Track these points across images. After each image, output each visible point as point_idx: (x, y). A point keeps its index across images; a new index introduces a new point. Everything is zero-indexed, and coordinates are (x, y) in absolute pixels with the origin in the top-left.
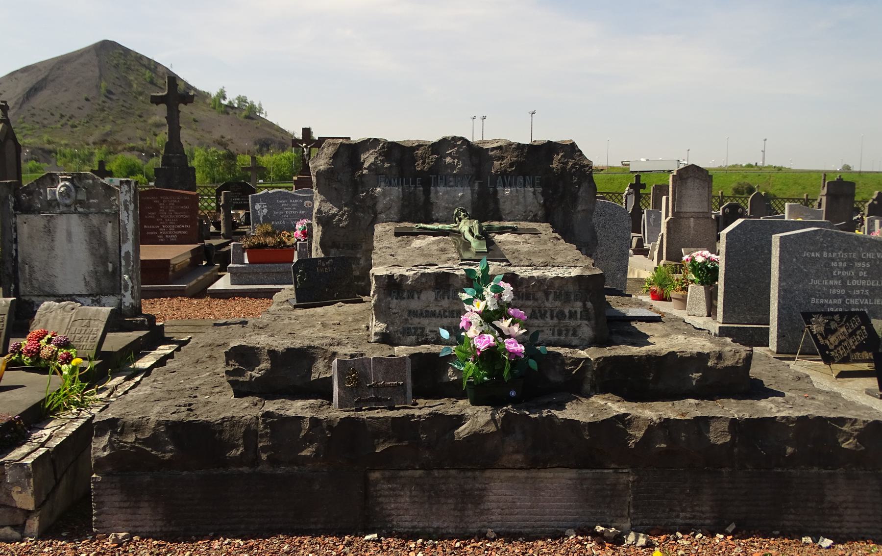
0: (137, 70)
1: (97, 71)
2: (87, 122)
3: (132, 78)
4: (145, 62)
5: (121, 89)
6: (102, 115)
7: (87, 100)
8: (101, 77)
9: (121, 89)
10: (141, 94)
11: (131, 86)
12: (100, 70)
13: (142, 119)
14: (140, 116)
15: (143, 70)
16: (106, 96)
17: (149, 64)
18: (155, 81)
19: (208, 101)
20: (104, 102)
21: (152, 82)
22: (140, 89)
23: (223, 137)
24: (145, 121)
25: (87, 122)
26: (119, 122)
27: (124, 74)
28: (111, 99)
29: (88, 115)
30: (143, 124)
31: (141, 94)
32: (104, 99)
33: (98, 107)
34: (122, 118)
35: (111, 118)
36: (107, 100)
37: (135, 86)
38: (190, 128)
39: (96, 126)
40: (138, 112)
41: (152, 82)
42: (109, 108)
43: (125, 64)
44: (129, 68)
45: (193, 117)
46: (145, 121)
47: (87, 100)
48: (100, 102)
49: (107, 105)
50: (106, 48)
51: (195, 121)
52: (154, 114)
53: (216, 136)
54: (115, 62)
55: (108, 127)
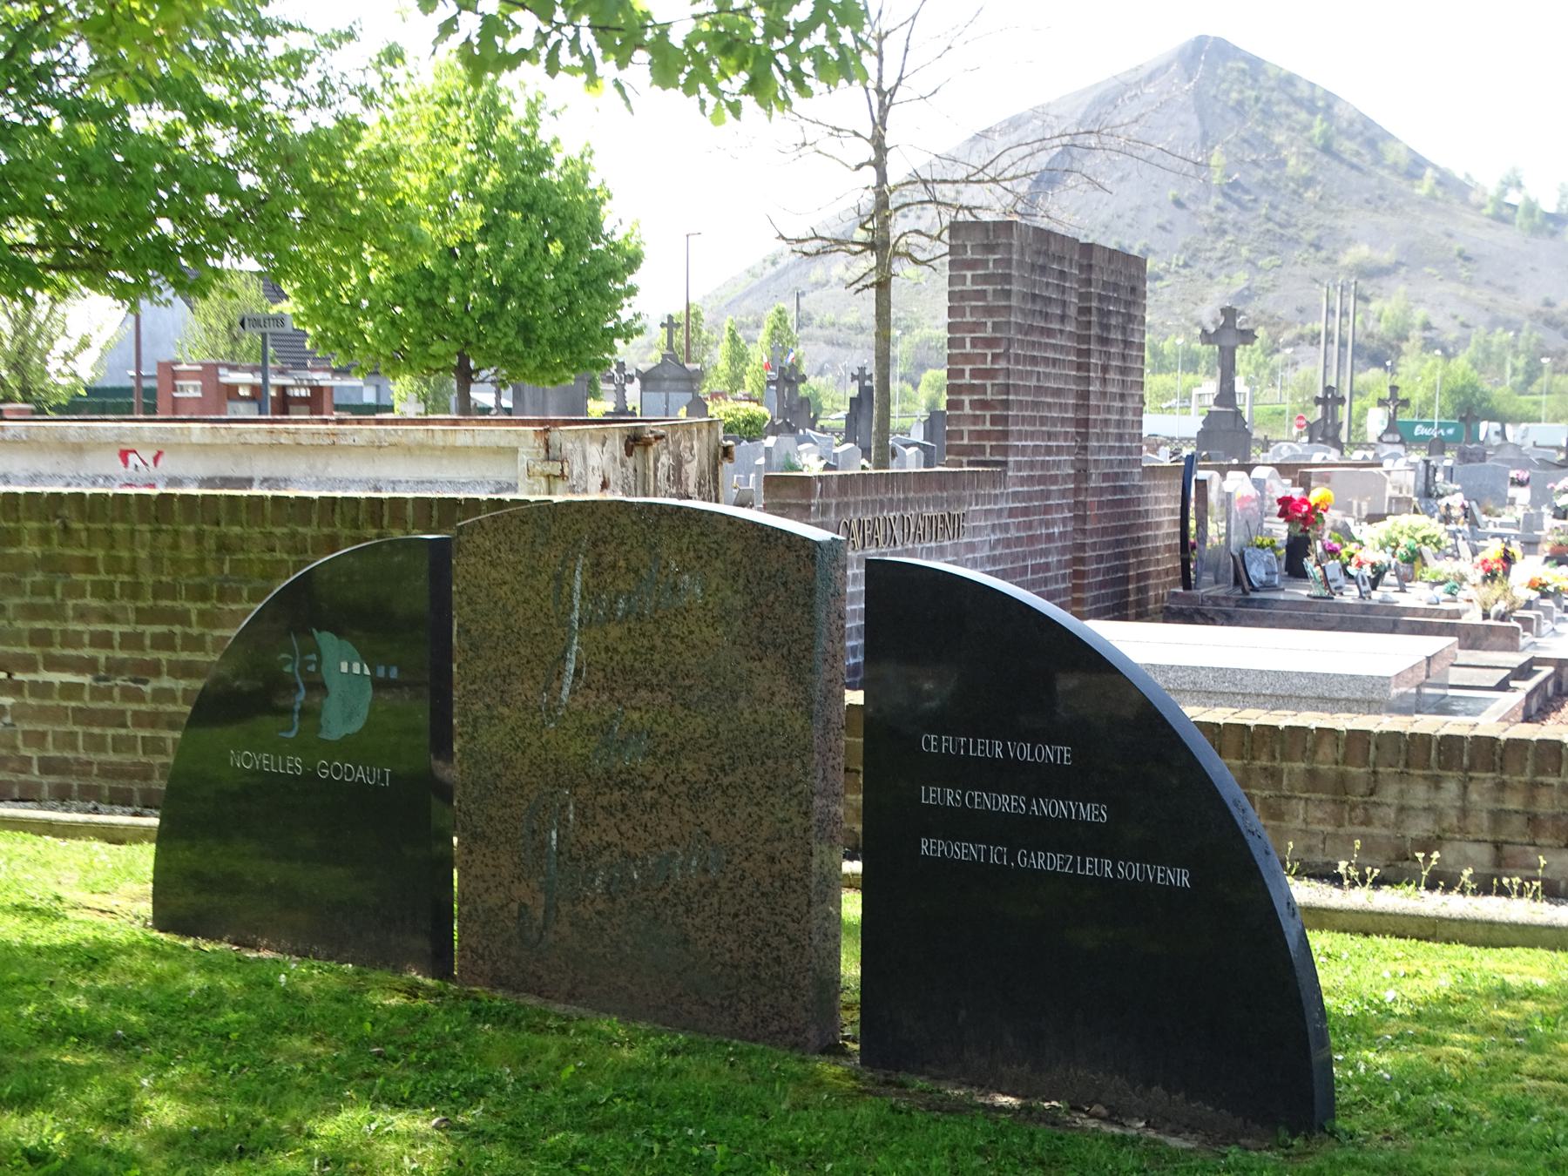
0: (1288, 116)
1: (1194, 121)
2: (1186, 265)
3: (1280, 138)
4: (1306, 92)
5: (1258, 174)
6: (1220, 244)
7: (1178, 203)
8: (1205, 136)
9: (1258, 174)
10: (1308, 182)
11: (1282, 163)
12: (1201, 120)
13: (1323, 254)
14: (1318, 248)
15: (1303, 116)
16: (1226, 195)
17: (1312, 101)
18: (1335, 146)
19: (1474, 197)
20: (1220, 208)
21: (1327, 149)
22: (1305, 170)
23: (1548, 304)
24: (1328, 260)
25: (1186, 265)
26: (1264, 262)
27: (1260, 129)
28: (1238, 202)
29: (1186, 246)
30: (1325, 268)
31: (1308, 182)
32: (1220, 200)
33: (1206, 222)
34: (1272, 253)
35: (1244, 251)
36: (1228, 204)
37: (1292, 162)
38: (1454, 277)
39: (1210, 276)
40: (1310, 235)
41: (1327, 149)
42: (1235, 224)
43: (1257, 99)
44: (1267, 113)
45: (1457, 247)
46: (1328, 260)
47: (1178, 203)
48: (1212, 209)
49: (1230, 216)
50: (1207, 55)
51: (1467, 259)
52: (1350, 241)
53: (1530, 300)
54: (1234, 95)
55: (1241, 279)
